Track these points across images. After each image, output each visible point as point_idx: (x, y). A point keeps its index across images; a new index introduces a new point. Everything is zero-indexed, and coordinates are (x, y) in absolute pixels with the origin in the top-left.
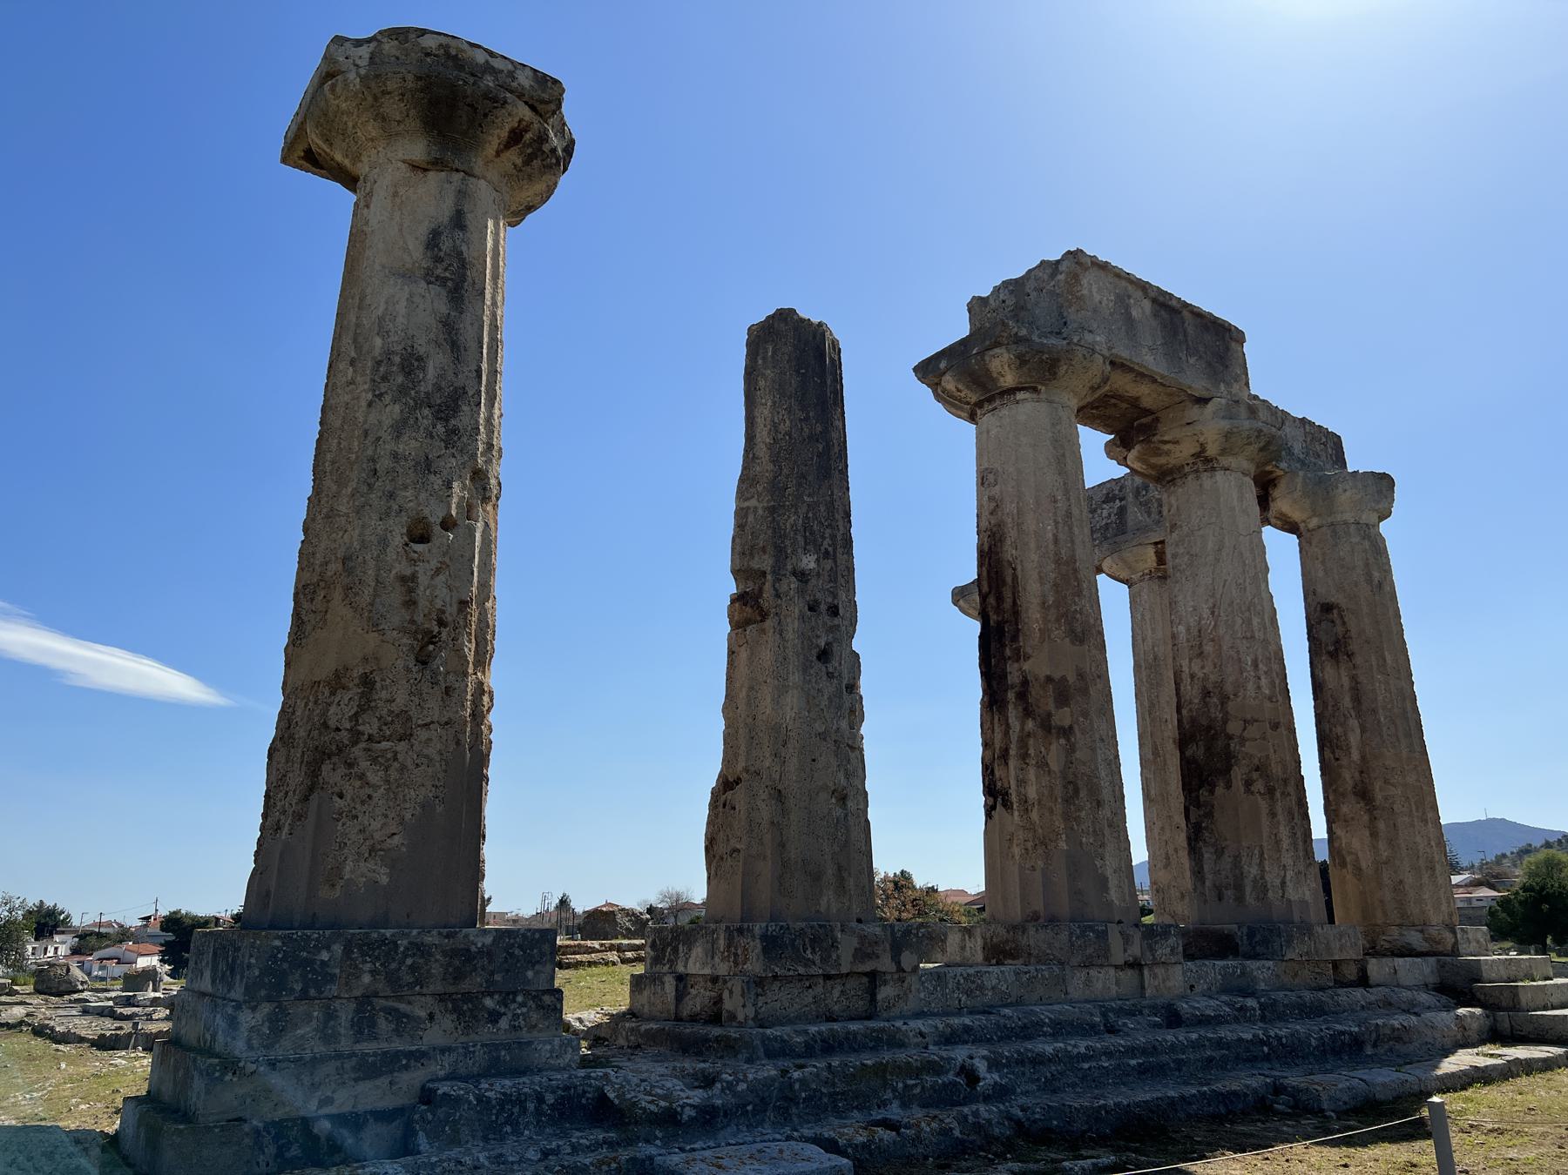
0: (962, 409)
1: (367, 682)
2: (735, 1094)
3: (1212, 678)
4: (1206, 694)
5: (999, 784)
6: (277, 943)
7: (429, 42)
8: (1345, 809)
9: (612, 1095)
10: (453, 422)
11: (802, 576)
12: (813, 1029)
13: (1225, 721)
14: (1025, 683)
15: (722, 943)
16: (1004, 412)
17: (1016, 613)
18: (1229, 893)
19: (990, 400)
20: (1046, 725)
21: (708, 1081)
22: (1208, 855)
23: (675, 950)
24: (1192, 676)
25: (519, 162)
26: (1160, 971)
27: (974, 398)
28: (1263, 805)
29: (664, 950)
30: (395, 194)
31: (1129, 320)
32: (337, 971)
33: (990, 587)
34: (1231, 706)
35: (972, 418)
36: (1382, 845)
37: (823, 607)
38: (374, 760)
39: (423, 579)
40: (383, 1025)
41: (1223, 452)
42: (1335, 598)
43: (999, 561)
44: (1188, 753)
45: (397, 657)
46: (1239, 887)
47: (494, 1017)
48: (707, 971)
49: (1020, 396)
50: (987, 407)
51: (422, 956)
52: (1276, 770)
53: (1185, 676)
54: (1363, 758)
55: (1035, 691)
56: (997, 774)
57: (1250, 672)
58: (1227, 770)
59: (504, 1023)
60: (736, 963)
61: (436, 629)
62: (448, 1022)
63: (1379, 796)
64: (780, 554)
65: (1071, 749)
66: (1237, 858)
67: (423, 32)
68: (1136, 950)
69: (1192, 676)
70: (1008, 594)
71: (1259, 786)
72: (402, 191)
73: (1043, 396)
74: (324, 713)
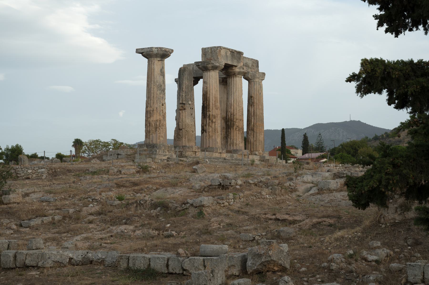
1: (160, 120)
3: (232, 112)
4: (231, 114)
7: (164, 49)
8: (250, 132)
11: (189, 104)
14: (210, 115)
16: (208, 73)
17: (209, 105)
18: (231, 145)
20: (212, 122)
28: (238, 132)
31: (227, 56)
34: (235, 117)
36: (255, 138)
42: (253, 95)
43: (207, 97)
45: (162, 118)
46: (233, 144)
52: (240, 127)
54: (254, 124)
55: (211, 116)
57: (238, 112)
63: (255, 131)
64: (188, 102)
65: (215, 125)
66: (233, 140)
67: (163, 48)
68: (221, 151)
70: (208, 102)
71: (237, 129)
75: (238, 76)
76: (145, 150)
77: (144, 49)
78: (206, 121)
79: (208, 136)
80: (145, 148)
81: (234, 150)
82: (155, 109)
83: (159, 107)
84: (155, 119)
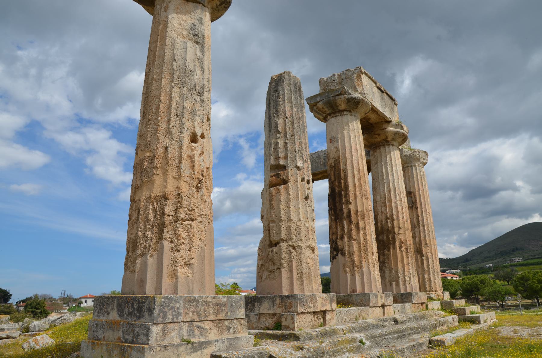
0: (322, 115)
2: (311, 352)
4: (387, 218)
5: (340, 247)
6: (163, 300)
9: (274, 355)
10: (202, 97)
11: (298, 168)
12: (318, 330)
13: (393, 227)
14: (349, 212)
15: (278, 301)
16: (339, 118)
18: (394, 283)
19: (334, 113)
21: (301, 348)
22: (387, 272)
24: (382, 213)
25: (218, 4)
26: (388, 307)
27: (328, 112)
30: (178, 8)
32: (182, 311)
33: (335, 178)
35: (325, 120)
37: (306, 180)
38: (184, 229)
39: (196, 158)
40: (197, 332)
41: (393, 139)
43: (339, 169)
44: (380, 238)
47: (229, 328)
48: (271, 311)
49: (345, 113)
50: (332, 115)
51: (207, 306)
53: (380, 213)
56: (339, 244)
58: (394, 243)
59: (231, 331)
60: (285, 308)
61: (201, 178)
62: (215, 330)
63: (424, 253)
69: (382, 213)
72: (180, 7)
73: (353, 114)
74: (163, 209)
75: (392, 142)
76: (112, 325)
78: (343, 227)
79: (349, 264)
80: (114, 315)
81: (402, 295)
82: (160, 152)
83: (175, 145)
84: (157, 191)
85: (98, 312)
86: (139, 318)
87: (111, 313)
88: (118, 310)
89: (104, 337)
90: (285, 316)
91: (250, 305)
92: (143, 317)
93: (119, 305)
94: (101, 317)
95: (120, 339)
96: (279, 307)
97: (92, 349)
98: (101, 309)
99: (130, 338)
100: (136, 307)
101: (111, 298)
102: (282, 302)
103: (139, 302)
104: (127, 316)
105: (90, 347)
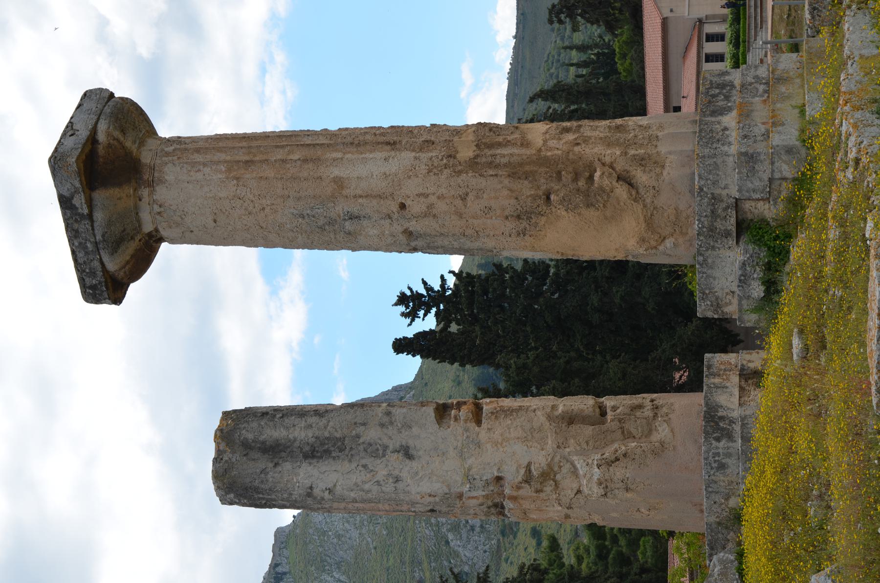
23: (722, 418)
29: (723, 429)
76: (745, 114)
77: (70, 125)
80: (730, 120)
85: (723, 145)
86: (733, 86)
87: (726, 124)
88: (721, 114)
89: (763, 123)
90: (745, 363)
91: (721, 425)
92: (731, 82)
93: (713, 113)
94: (732, 139)
95: (765, 101)
96: (728, 379)
97: (783, 124)
98: (718, 140)
99: (761, 88)
100: (717, 91)
101: (702, 126)
102: (719, 375)
103: (711, 88)
104: (729, 101)
105: (780, 128)
